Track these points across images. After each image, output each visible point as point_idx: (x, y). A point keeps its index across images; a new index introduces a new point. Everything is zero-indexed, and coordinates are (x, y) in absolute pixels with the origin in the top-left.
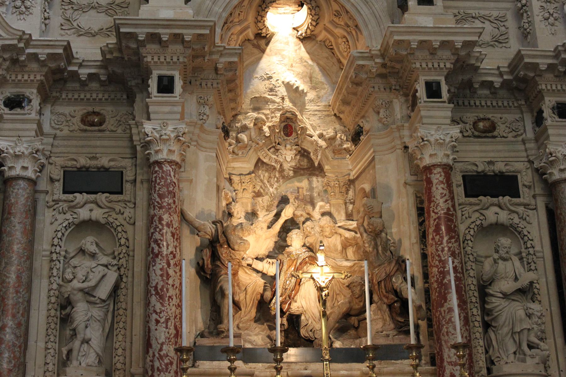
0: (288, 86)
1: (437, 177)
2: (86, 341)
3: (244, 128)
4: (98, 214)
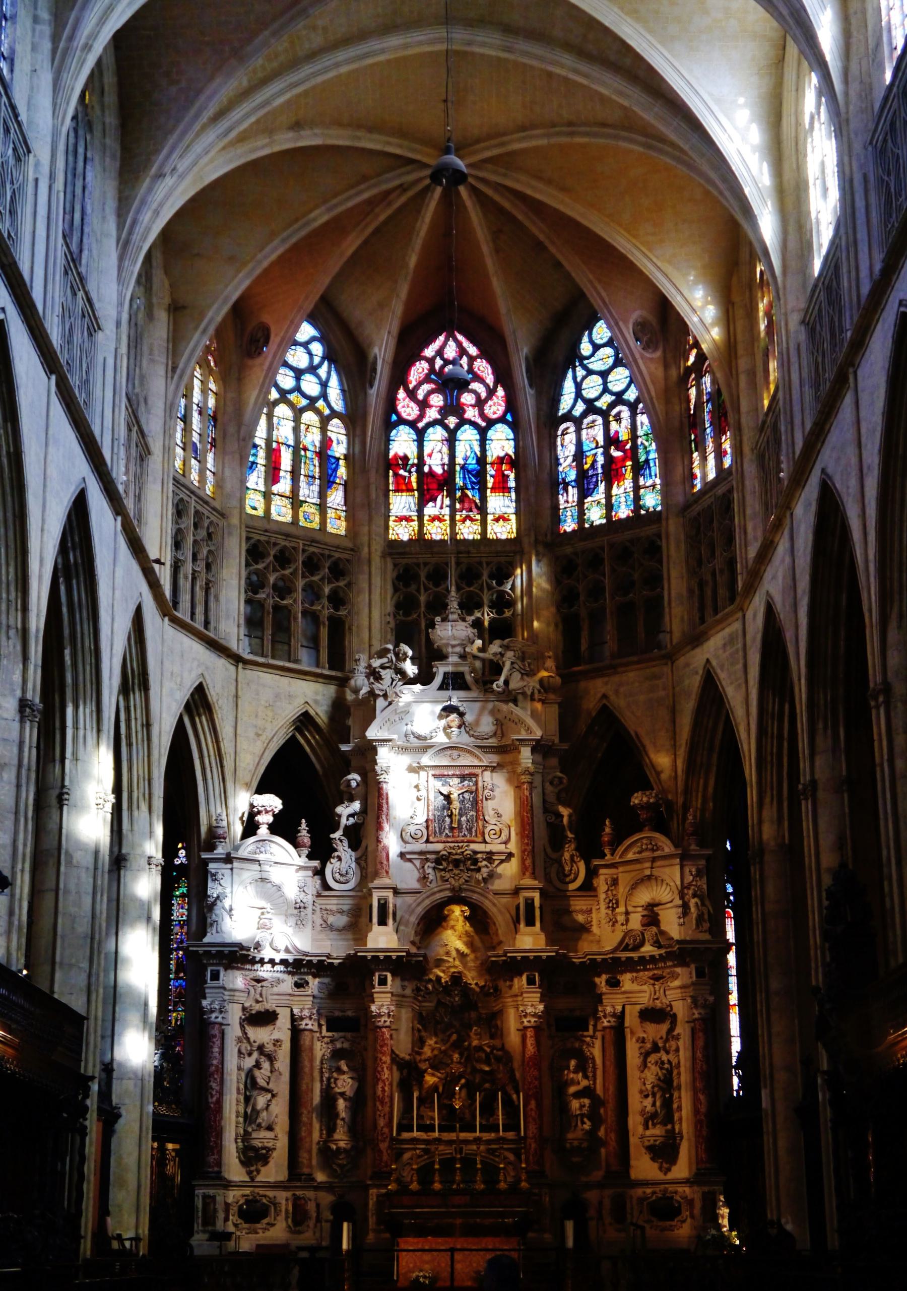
0: (457, 951)
1: (530, 1033)
2: (343, 1119)
3: (431, 980)
4: (346, 1045)
